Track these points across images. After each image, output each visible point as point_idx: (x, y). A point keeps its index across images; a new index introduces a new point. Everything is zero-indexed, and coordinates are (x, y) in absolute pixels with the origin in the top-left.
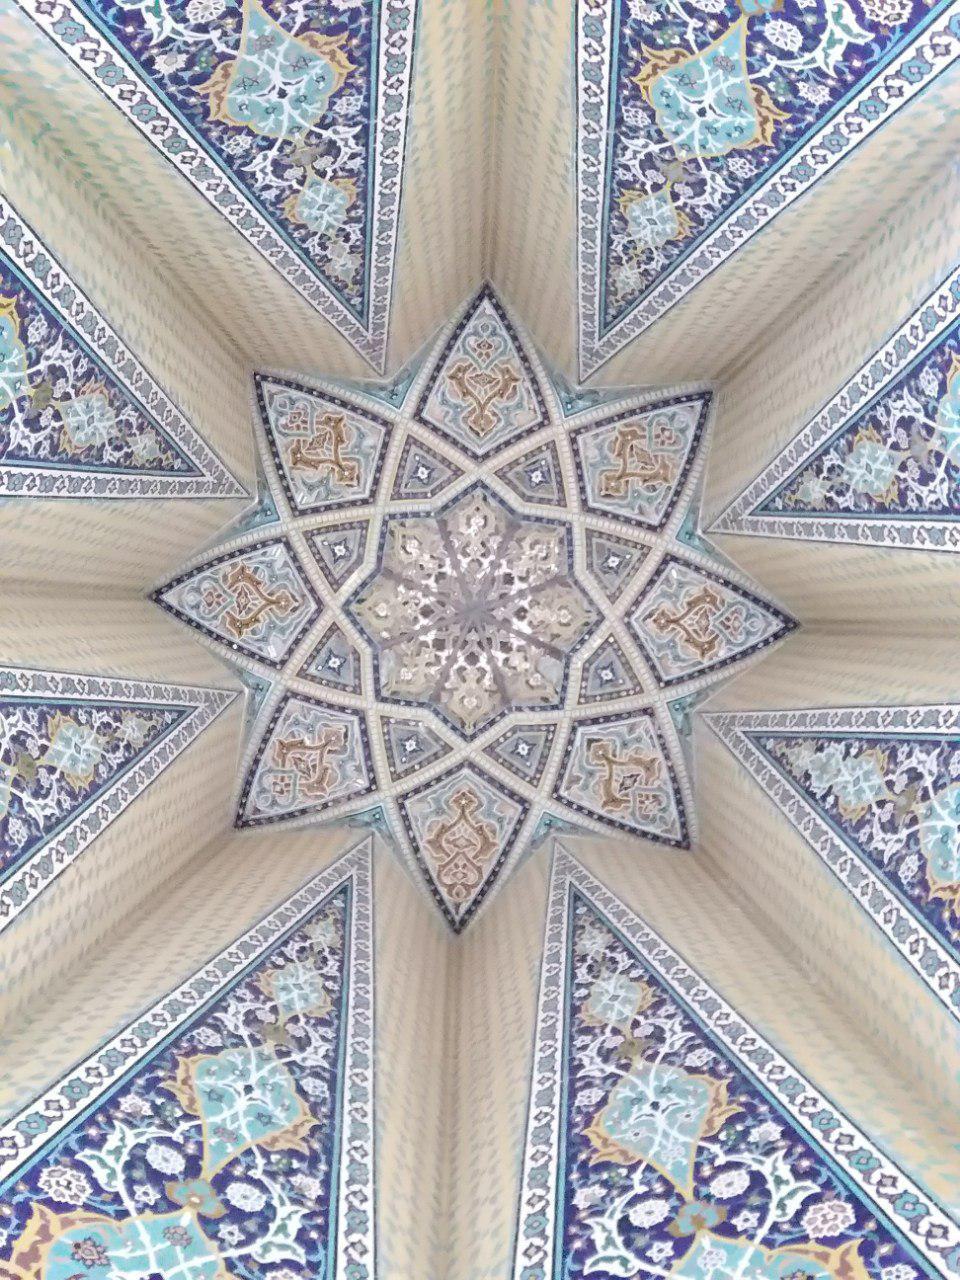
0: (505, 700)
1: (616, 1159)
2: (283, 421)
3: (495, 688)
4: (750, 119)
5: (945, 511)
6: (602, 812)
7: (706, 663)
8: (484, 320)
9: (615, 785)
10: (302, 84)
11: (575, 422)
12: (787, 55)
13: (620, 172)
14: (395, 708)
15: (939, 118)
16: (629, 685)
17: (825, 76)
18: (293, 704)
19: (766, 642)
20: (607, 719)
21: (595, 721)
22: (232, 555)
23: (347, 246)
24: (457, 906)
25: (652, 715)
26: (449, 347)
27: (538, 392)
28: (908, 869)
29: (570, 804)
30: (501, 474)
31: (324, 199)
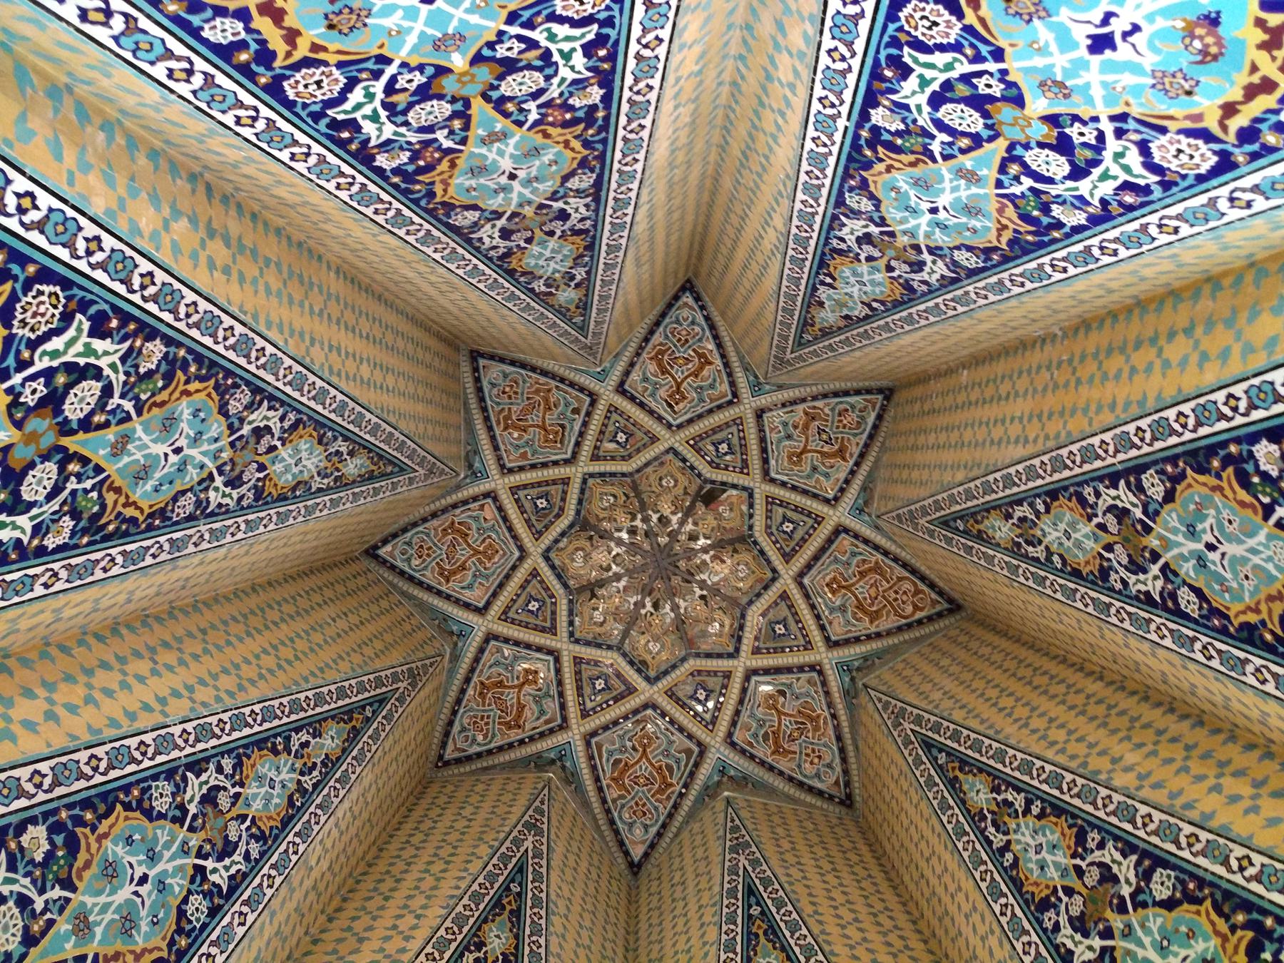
0: (742, 539)
2: (480, 738)
3: (730, 548)
4: (184, 409)
5: (597, 199)
6: (851, 462)
7: (718, 362)
8: (397, 553)
9: (826, 449)
10: (133, 860)
11: (493, 469)
12: (107, 391)
13: (245, 503)
14: (745, 641)
15: (182, 225)
16: (734, 429)
17: (131, 349)
18: (737, 738)
19: (702, 308)
20: (764, 450)
21: (765, 461)
22: (600, 789)
23: (313, 742)
24: (934, 603)
25: (763, 411)
26: (420, 584)
27: (465, 502)
29: (842, 490)
30: (538, 535)
31: (262, 786)
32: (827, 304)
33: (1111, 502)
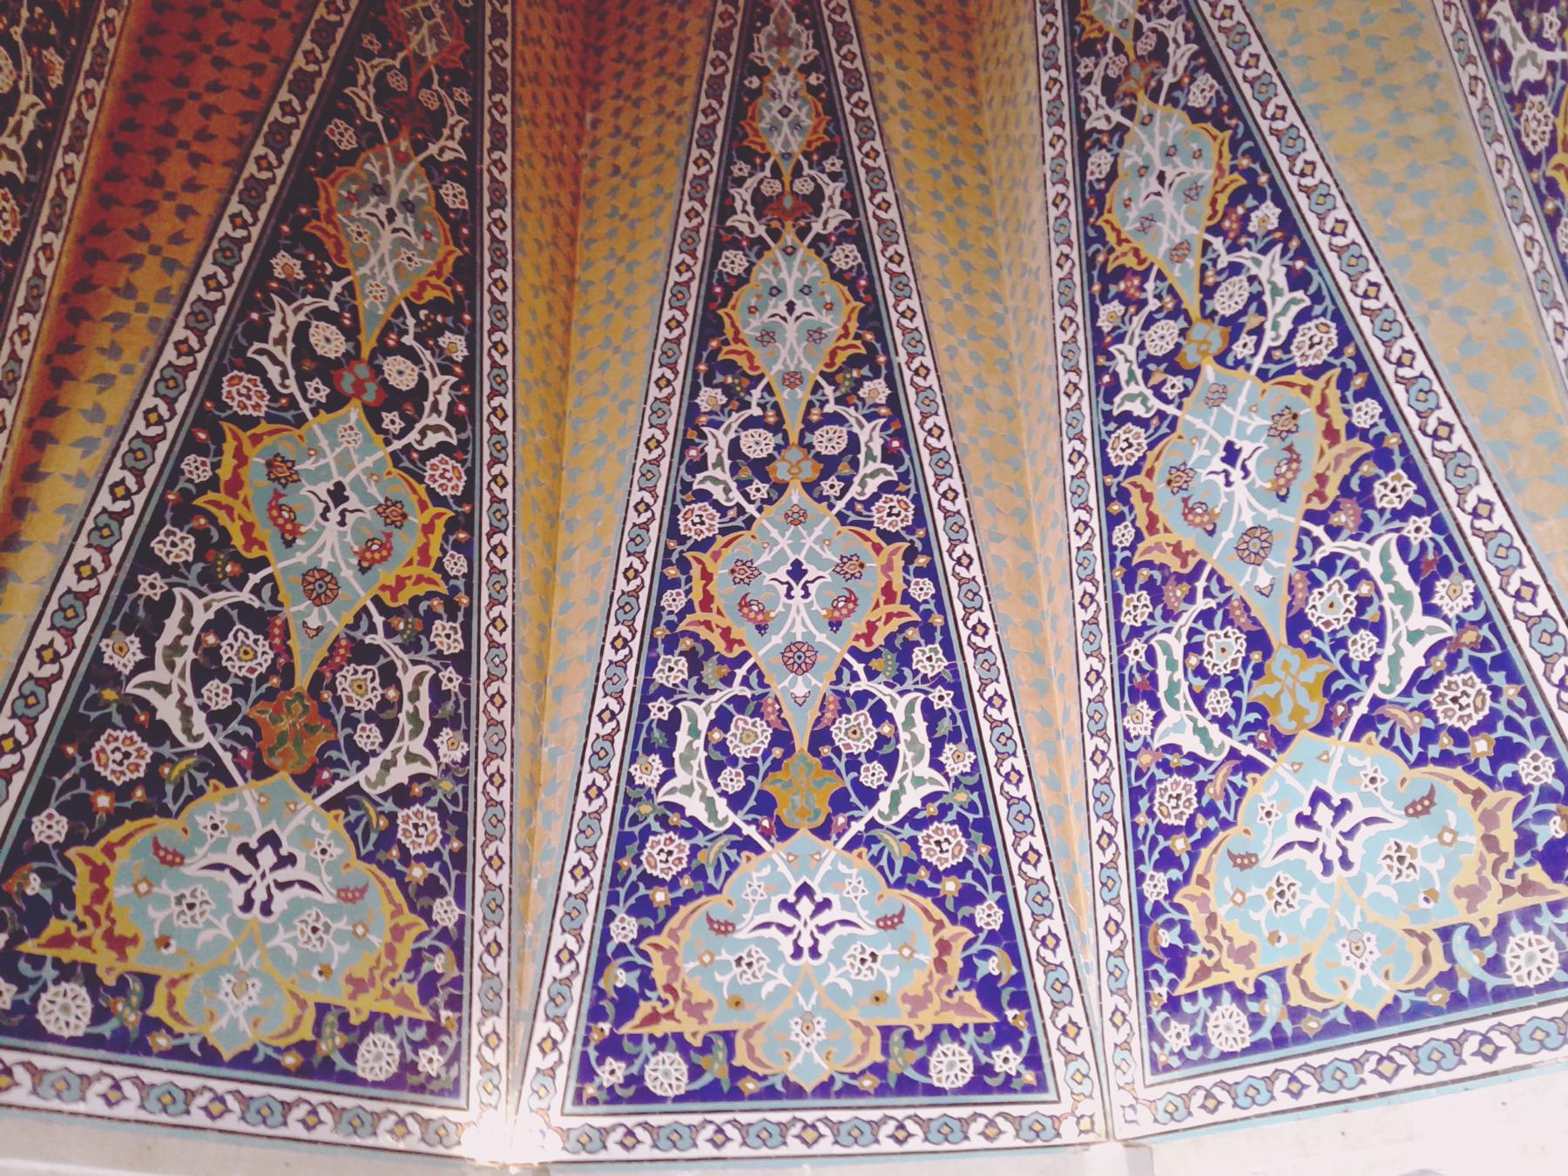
1: (330, 246)
5: (1081, 123)
28: (733, 262)
32: (795, 26)
33: (451, 121)
